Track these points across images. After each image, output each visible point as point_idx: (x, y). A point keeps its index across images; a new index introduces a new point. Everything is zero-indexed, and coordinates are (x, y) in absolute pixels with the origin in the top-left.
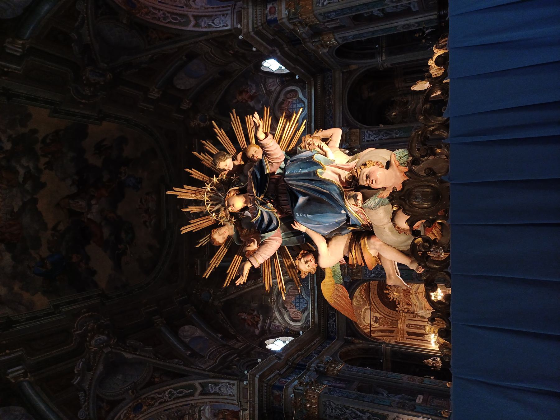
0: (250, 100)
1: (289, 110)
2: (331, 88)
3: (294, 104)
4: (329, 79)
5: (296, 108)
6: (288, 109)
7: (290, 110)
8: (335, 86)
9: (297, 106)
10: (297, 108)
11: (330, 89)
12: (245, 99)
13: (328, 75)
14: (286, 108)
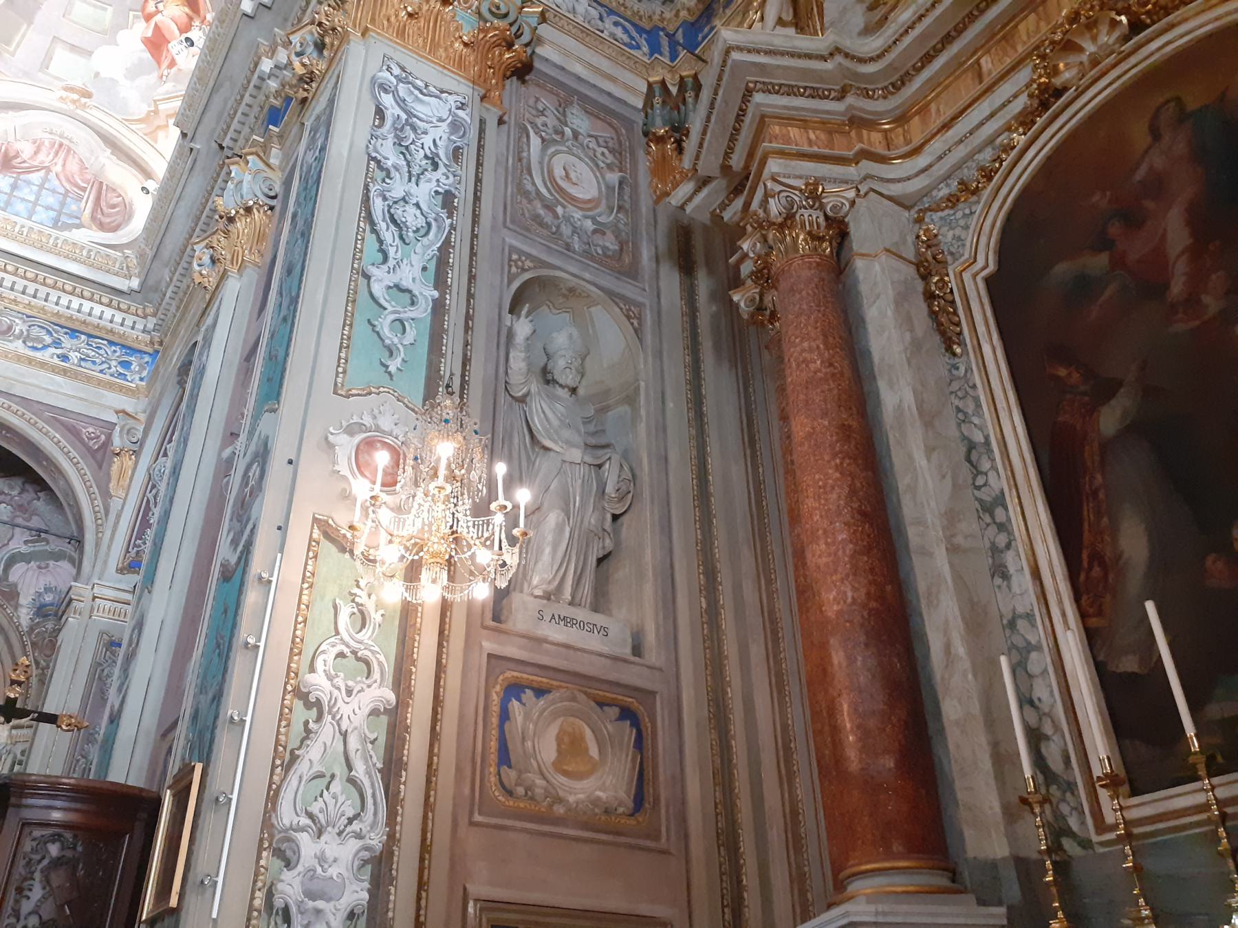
0: (149, 34)
1: (42, 173)
2: (64, 358)
3: (63, 204)
4: (114, 363)
5: (37, 199)
6: (48, 169)
7: (36, 177)
8: (64, 372)
9: (48, 208)
10: (35, 204)
11: (59, 351)
12: (158, 12)
13: (135, 367)
14: (58, 168)
